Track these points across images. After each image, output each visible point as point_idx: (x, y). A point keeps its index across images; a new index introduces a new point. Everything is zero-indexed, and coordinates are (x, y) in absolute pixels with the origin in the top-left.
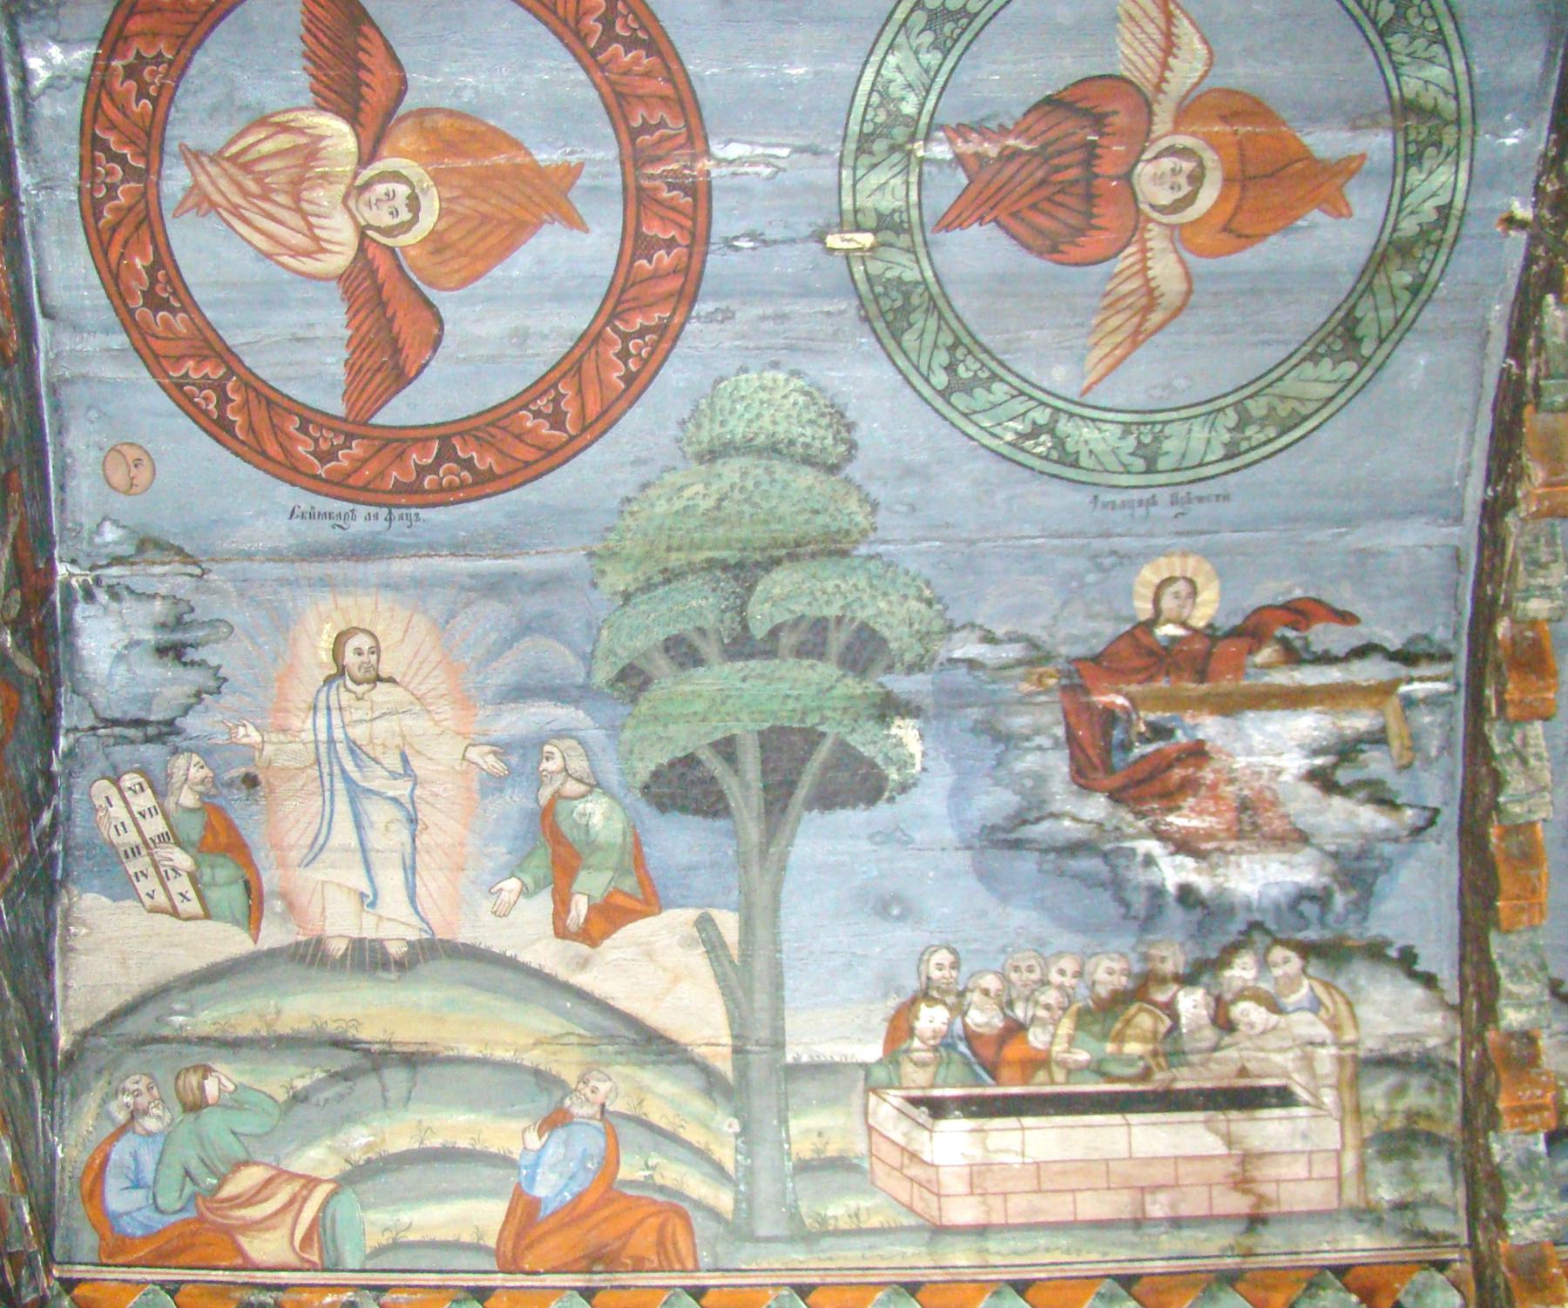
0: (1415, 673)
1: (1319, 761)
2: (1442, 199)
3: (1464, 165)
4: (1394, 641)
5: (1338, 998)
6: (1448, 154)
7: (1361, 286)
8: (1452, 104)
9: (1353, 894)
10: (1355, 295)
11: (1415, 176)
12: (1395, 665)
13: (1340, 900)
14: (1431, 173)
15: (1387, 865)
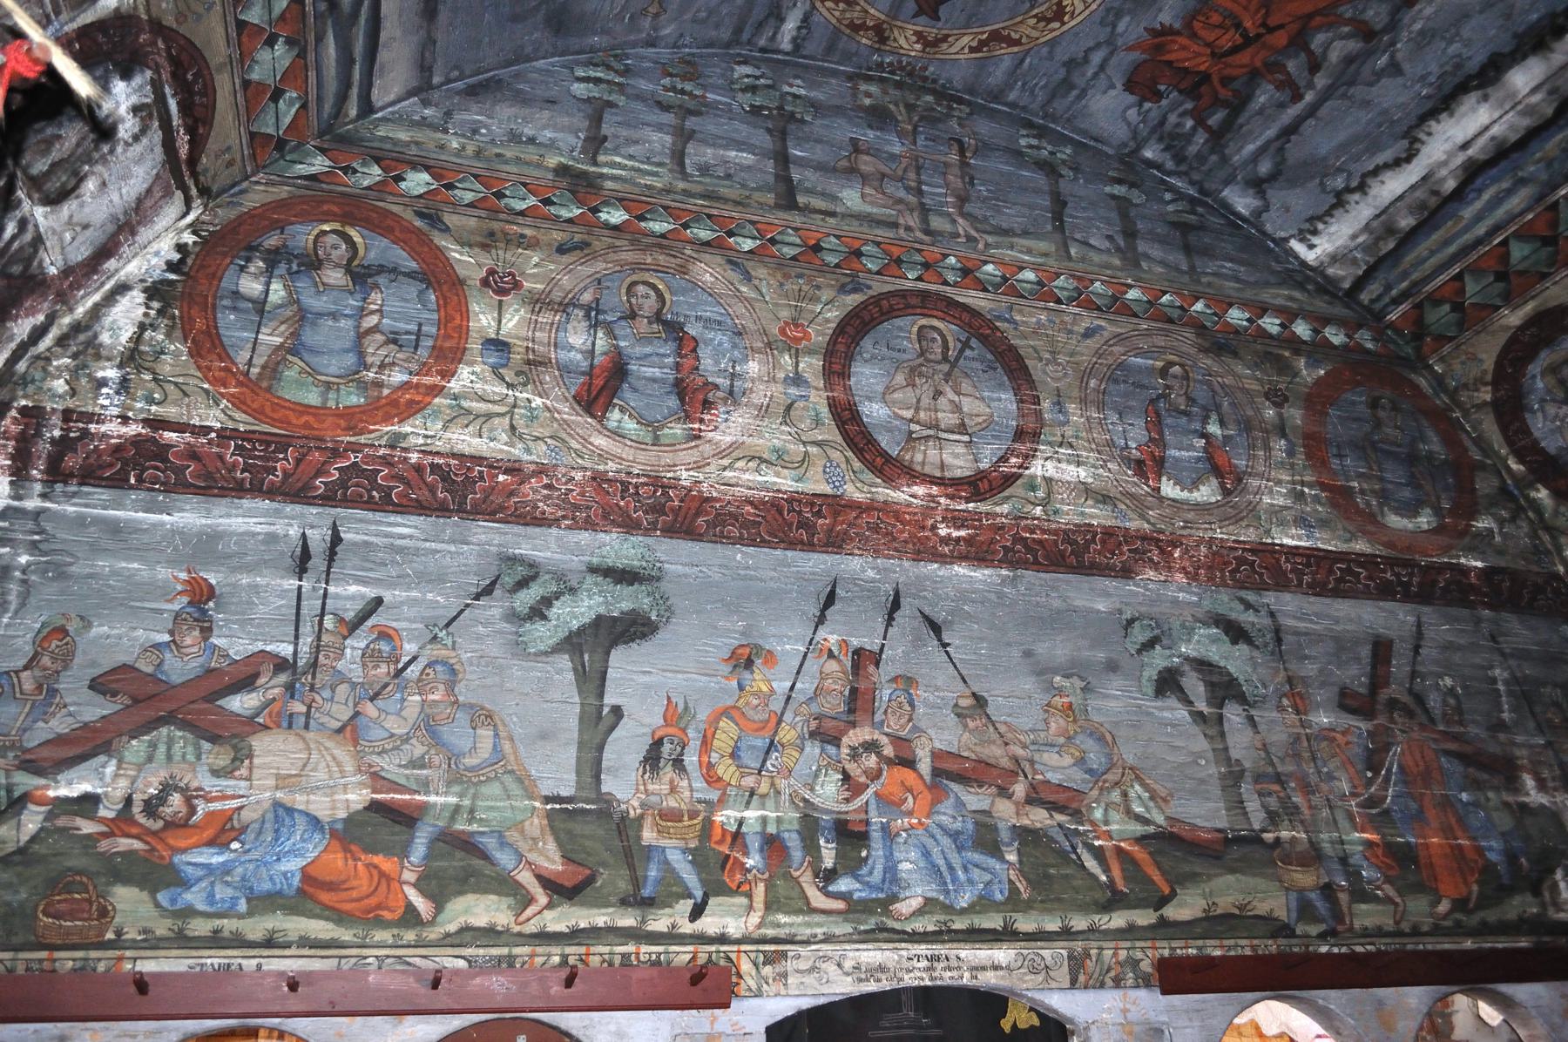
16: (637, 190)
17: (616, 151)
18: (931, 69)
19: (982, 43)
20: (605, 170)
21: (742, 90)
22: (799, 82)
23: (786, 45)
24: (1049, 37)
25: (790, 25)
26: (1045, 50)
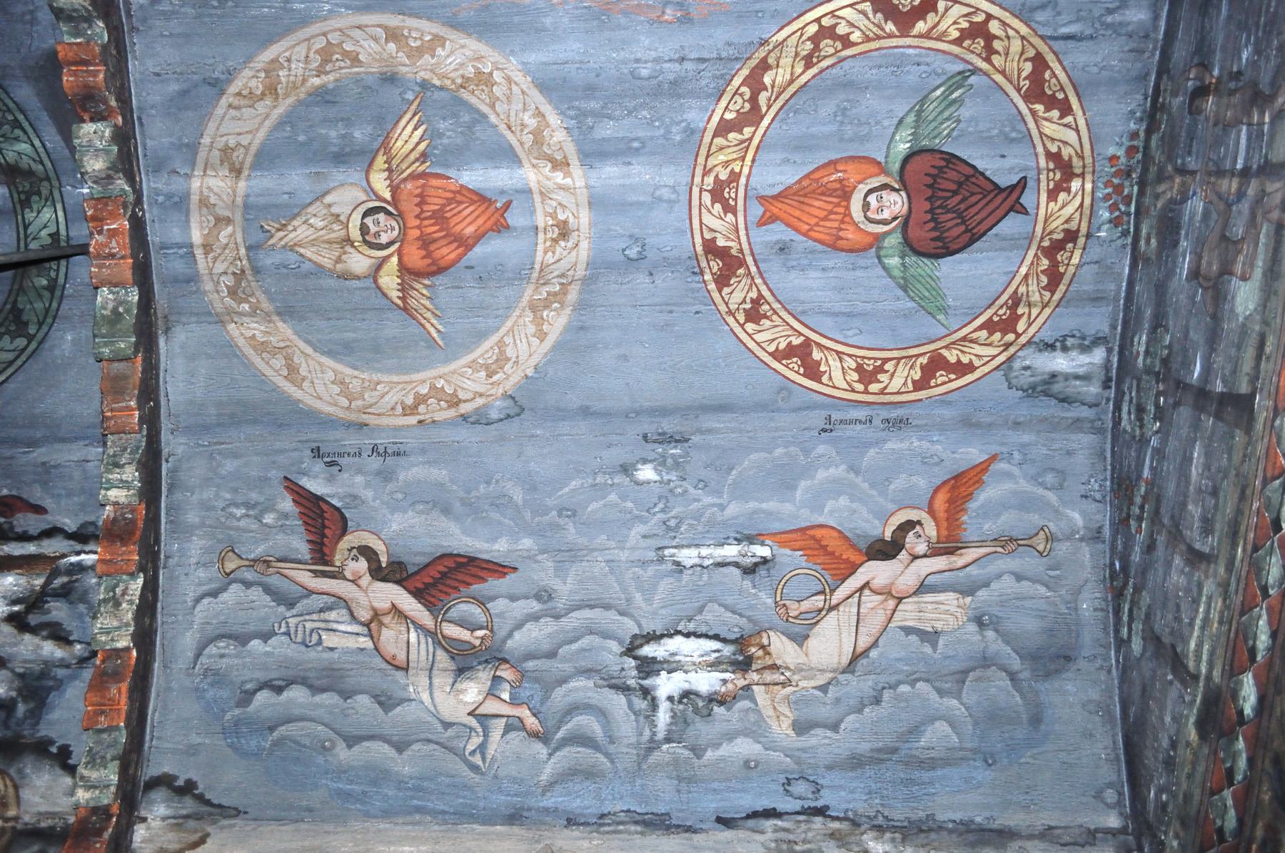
0: (87, 548)
1: (16, 608)
2: (52, 229)
3: (59, 206)
4: (70, 524)
5: (8, 782)
6: (47, 200)
7: (16, 287)
8: (40, 167)
9: (32, 705)
10: (14, 293)
11: (30, 216)
12: (72, 542)
13: (21, 708)
14: (39, 212)
15: (59, 685)
16: (1223, 639)
17: (1187, 643)
18: (1111, 151)
19: (1051, 103)
20: (1204, 671)
21: (1141, 427)
22: (1136, 340)
23: (1098, 355)
24: (1016, 23)
25: (1061, 363)
26: (1041, 16)
